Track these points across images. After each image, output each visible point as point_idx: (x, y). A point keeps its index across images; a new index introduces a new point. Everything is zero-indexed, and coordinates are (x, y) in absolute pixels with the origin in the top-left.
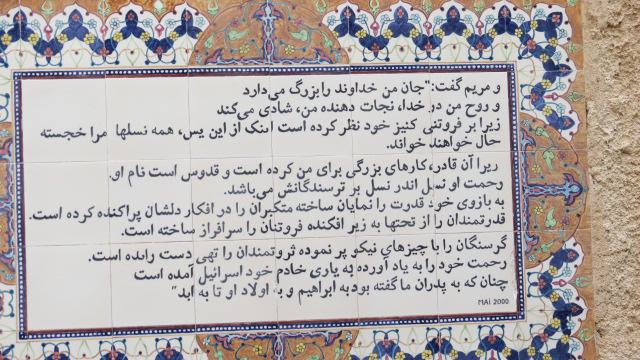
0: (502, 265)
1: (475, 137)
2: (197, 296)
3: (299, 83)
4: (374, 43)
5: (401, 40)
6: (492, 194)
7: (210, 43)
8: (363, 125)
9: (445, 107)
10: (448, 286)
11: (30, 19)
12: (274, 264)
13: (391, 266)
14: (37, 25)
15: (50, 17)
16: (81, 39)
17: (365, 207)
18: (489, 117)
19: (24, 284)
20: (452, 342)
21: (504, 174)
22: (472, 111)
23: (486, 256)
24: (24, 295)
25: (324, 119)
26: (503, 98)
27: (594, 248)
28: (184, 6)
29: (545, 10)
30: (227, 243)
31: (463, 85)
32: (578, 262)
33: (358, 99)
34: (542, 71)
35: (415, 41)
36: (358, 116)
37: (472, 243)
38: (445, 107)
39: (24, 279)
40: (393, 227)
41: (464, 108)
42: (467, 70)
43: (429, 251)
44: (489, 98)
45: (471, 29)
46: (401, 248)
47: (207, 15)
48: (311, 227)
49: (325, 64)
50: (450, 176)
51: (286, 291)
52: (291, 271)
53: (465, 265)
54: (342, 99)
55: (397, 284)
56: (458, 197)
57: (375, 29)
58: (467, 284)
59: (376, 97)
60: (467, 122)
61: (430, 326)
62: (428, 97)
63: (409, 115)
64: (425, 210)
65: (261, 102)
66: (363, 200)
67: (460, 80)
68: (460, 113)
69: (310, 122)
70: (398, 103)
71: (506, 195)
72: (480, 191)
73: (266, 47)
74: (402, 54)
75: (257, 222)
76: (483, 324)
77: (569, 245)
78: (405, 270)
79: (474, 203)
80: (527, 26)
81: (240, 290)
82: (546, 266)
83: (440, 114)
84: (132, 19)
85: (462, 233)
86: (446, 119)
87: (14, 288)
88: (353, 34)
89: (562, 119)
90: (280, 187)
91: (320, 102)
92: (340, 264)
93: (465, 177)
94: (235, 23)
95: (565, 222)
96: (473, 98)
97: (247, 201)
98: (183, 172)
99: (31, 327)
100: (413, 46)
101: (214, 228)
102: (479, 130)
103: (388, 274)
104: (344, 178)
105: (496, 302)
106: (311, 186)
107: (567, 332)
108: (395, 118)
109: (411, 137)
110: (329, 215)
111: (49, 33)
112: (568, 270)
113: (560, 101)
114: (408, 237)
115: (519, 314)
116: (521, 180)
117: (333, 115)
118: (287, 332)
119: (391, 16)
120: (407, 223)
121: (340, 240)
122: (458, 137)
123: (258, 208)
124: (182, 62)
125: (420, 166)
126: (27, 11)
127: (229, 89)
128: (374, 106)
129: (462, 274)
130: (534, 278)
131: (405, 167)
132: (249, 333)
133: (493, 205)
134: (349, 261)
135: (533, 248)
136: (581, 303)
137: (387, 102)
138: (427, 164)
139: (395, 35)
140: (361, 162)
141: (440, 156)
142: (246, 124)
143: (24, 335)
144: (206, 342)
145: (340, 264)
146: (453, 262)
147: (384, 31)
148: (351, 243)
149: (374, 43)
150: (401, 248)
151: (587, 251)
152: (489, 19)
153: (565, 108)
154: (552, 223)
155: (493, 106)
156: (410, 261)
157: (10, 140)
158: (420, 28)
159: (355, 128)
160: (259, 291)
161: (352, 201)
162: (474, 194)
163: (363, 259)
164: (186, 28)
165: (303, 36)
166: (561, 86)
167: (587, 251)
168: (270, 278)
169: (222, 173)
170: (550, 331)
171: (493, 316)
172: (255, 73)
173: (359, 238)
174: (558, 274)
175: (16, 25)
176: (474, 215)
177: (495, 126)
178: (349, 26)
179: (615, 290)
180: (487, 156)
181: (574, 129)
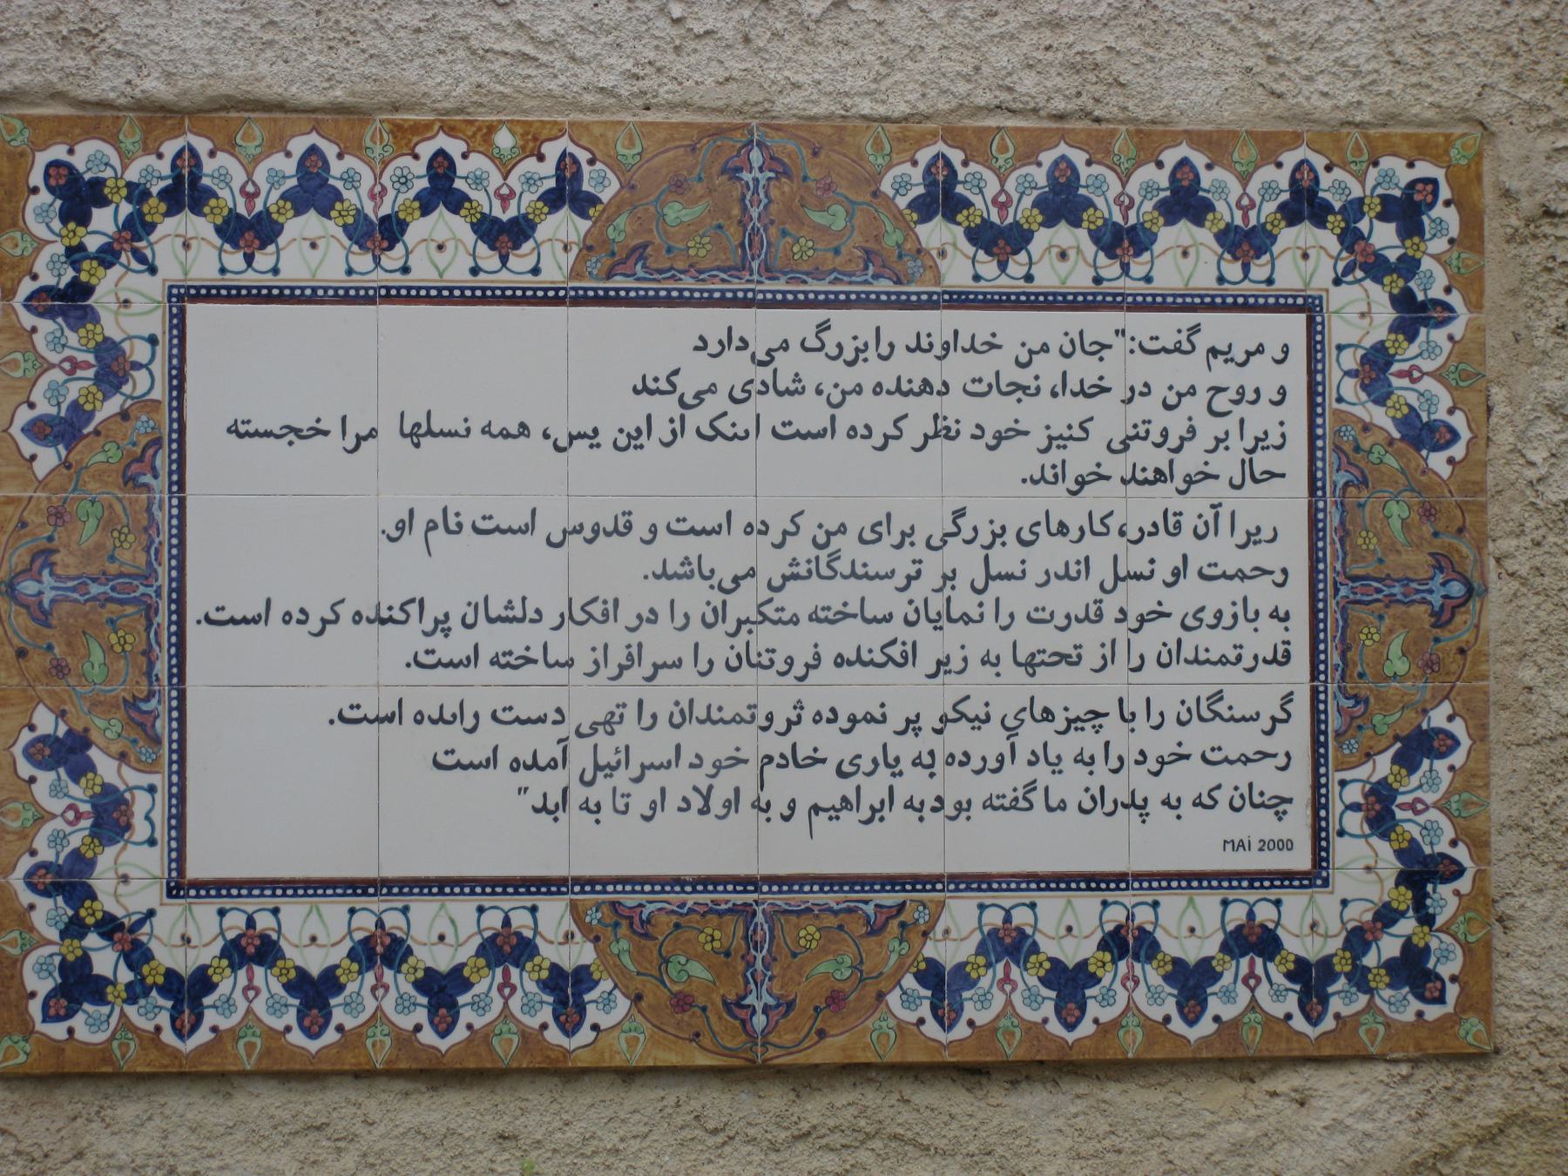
0: (1282, 761)
1: (1227, 464)
3: (824, 327)
5: (1063, 234)
6: (1262, 594)
7: (621, 230)
8: (967, 429)
9: (1159, 392)
10: (1154, 807)
11: (209, 165)
12: (748, 740)
13: (1023, 755)
14: (224, 177)
15: (256, 160)
16: (325, 213)
17: (966, 619)
18: (1260, 418)
19: (182, 773)
20: (1159, 935)
21: (1292, 552)
22: (1221, 403)
23: (1246, 739)
24: (179, 798)
25: (878, 412)
26: (1295, 375)
27: (1498, 724)
28: (564, 143)
29: (1399, 173)
30: (647, 693)
31: (1203, 342)
32: (1458, 758)
33: (960, 368)
34: (1385, 314)
35: (1095, 237)
36: (956, 407)
37: (1211, 709)
38: (1159, 392)
39: (182, 761)
40: (1030, 665)
41: (1203, 396)
42: (1212, 307)
43: (1112, 724)
44: (1262, 374)
45: (1225, 212)
46: (1048, 715)
47: (615, 165)
48: (840, 661)
49: (884, 285)
50: (1166, 551)
51: (780, 807)
52: (792, 760)
53: (1196, 759)
54: (923, 367)
55: (1037, 797)
56: (1183, 599)
57: (1003, 207)
58: (1198, 803)
59: (1002, 363)
60: (1209, 428)
61: (1110, 896)
62: (1118, 369)
63: (1073, 409)
64: (1108, 629)
65: (735, 369)
66: (964, 602)
67: (1195, 329)
68: (1194, 406)
69: (845, 419)
70: (1050, 380)
71: (1296, 598)
72: (1236, 589)
73: (749, 242)
74: (1063, 268)
75: (717, 644)
76: (1231, 895)
77: (1438, 717)
78: (1055, 766)
79: (1219, 615)
80: (1355, 209)
81: (673, 801)
82: (1383, 766)
83: (1145, 408)
84: (441, 168)
85: (1192, 682)
86: (1161, 419)
87: (156, 779)
88: (951, 217)
89: (1431, 427)
90: (773, 565)
91: (871, 371)
92: (905, 748)
93: (1201, 554)
94: (678, 187)
95: (1431, 666)
96: (1224, 373)
97: (694, 597)
99: (194, 871)
100: (1089, 248)
101: (618, 656)
102: (1237, 447)
104: (920, 551)
105: (1264, 845)
106: (843, 566)
107: (1426, 920)
109: (1080, 458)
110: (883, 633)
111: (250, 197)
112: (1432, 781)
113: (1428, 384)
115: (1317, 875)
116: (1331, 565)
117: (899, 404)
118: (781, 900)
119: (1040, 176)
120: (1063, 657)
122: (1188, 462)
123: (720, 613)
124: (555, 271)
125: (1098, 527)
126: (202, 146)
128: (995, 386)
129: (1187, 780)
130: (1354, 794)
131: (1063, 529)
132: (691, 899)
133: (1264, 621)
134: (928, 740)
135: (1354, 724)
136: (1461, 854)
137: (1024, 377)
138: (1114, 523)
139: (1049, 223)
140: (960, 513)
141: (1145, 506)
142: (698, 418)
143: (178, 888)
144: (593, 918)
145: (905, 748)
147: (1024, 209)
148: (933, 701)
150: (1048, 715)
151: (1480, 734)
152: (1268, 189)
153: (1439, 403)
154: (1401, 666)
155: (1270, 393)
156: (1067, 746)
157: (157, 442)
158: (1106, 208)
159: (950, 435)
160: (716, 806)
161: (936, 604)
162: (1221, 596)
163: (959, 737)
165: (836, 218)
166: (1430, 350)
167: (1480, 734)
168: (745, 777)
169: (640, 529)
170: (1386, 916)
171: (1255, 879)
172: (723, 302)
173: (952, 689)
174: (1411, 786)
175: (178, 179)
176: (1218, 643)
177: (1275, 439)
179: (1541, 825)
180: (1254, 508)
181: (1458, 451)
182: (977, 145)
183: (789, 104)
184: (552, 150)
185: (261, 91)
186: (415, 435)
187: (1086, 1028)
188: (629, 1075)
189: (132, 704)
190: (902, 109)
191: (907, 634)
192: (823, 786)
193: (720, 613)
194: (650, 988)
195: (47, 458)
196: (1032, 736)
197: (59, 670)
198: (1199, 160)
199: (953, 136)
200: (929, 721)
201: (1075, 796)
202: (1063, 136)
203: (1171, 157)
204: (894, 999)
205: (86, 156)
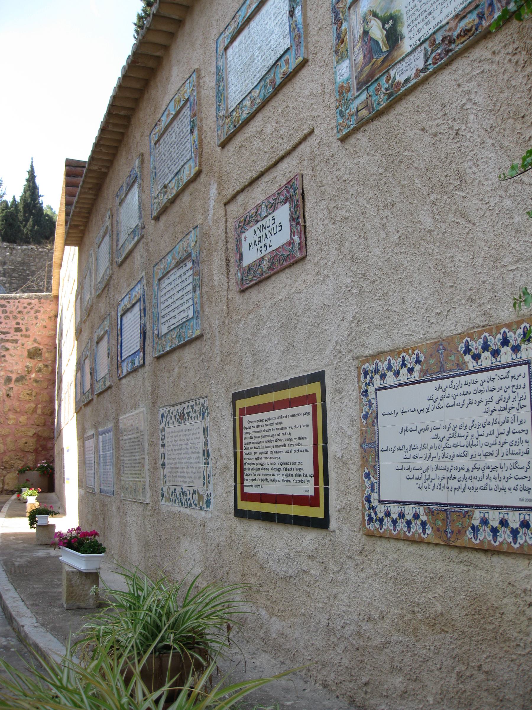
0: (528, 479)
1: (516, 404)
2: (423, 489)
3: (452, 382)
8: (474, 402)
10: (507, 490)
20: (509, 522)
22: (514, 390)
25: (460, 399)
30: (432, 463)
31: (510, 375)
37: (515, 466)
38: (504, 388)
40: (485, 456)
41: (511, 388)
45: (512, 343)
46: (488, 468)
47: (424, 354)
49: (460, 371)
50: (506, 426)
51: (450, 489)
53: (513, 478)
54: (465, 389)
60: (513, 396)
62: (497, 384)
63: (489, 395)
64: (498, 447)
65: (440, 393)
67: (509, 372)
68: (509, 391)
70: (486, 388)
79: (516, 442)
83: (502, 392)
84: (403, 360)
85: (510, 460)
91: (460, 391)
96: (515, 382)
97: (437, 442)
98: (419, 430)
100: (490, 356)
102: (518, 399)
103: (485, 481)
108: (486, 396)
109: (492, 406)
114: (492, 462)
119: (481, 341)
121: (467, 463)
123: (440, 446)
124: (417, 378)
127: (429, 388)
129: (512, 483)
133: (524, 444)
138: (497, 421)
140: (473, 421)
141: (501, 416)
142: (436, 404)
143: (380, 501)
146: (507, 476)
149: (476, 357)
155: (522, 386)
156: (492, 475)
164: (418, 361)
165: (452, 358)
168: (444, 481)
169: (430, 430)
173: (474, 461)
176: (515, 449)
177: (524, 397)
178: (467, 351)
183: (445, 334)
184: (415, 352)
185: (382, 350)
186: (403, 412)
187: (497, 543)
188: (429, 544)
189: (374, 466)
190: (459, 331)
191: (467, 449)
192: (454, 484)
193: (440, 446)
194: (434, 526)
195: (365, 421)
196: (487, 472)
197: (367, 461)
198: (507, 330)
199: (468, 335)
200: (471, 469)
201: (494, 487)
202: (485, 331)
203: (502, 331)
204: (468, 532)
205: (366, 366)
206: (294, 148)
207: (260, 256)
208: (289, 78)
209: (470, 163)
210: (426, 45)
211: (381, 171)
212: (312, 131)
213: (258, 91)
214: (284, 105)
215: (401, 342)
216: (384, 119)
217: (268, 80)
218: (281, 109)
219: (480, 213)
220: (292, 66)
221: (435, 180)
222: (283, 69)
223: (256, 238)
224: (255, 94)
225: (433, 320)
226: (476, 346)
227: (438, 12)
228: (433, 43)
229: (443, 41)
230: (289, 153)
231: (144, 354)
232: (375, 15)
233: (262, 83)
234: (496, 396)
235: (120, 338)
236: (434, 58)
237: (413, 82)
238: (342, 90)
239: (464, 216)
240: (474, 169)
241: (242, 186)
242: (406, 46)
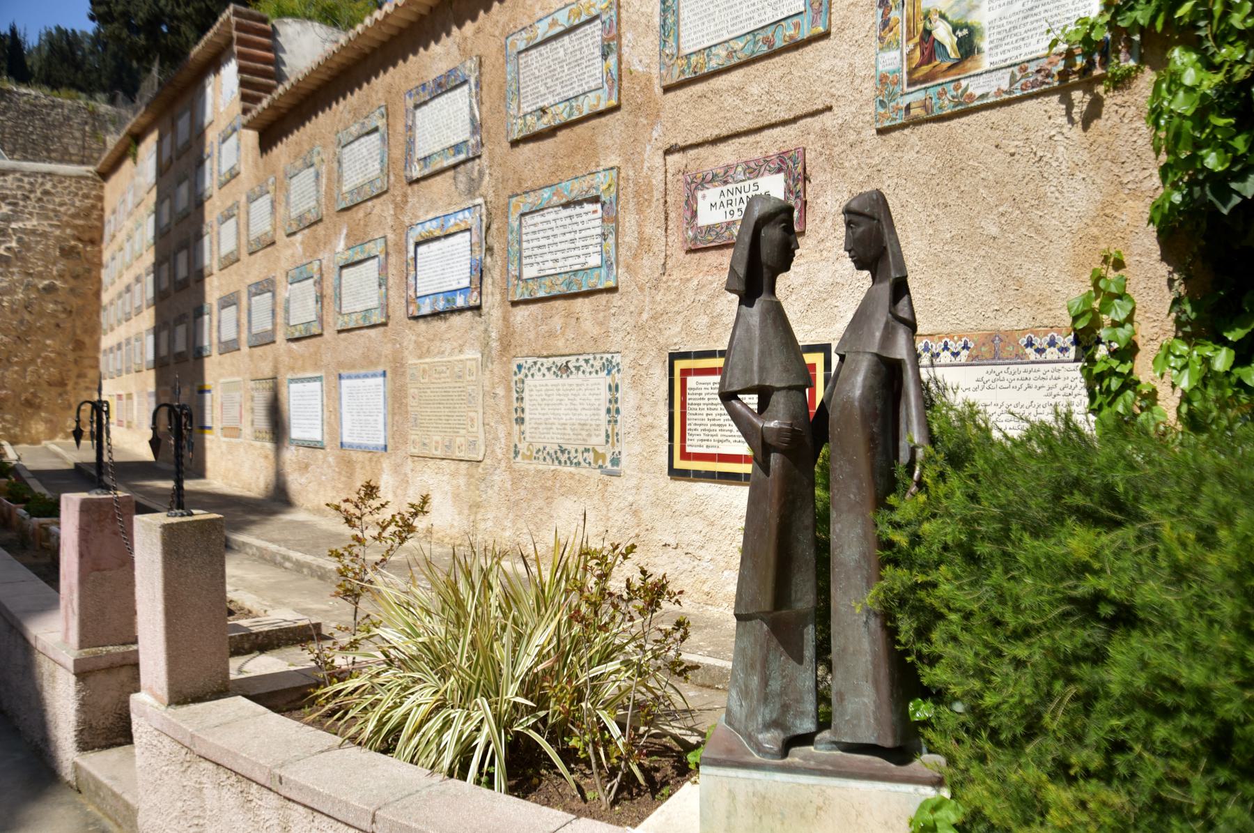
4: (1040, 351)
5: (1052, 349)
7: (974, 353)
25: (1018, 384)
33: (1033, 375)
36: (1032, 382)
54: (1025, 375)
59: (1040, 374)
62: (1063, 374)
63: (1053, 382)
65: (993, 376)
73: (996, 353)
83: (1068, 381)
84: (946, 344)
90: (999, 411)
91: (1016, 376)
108: (1047, 383)
109: (1054, 391)
122: (1076, 392)
124: (963, 361)
147: (1045, 345)
149: (1040, 351)
164: (965, 347)
165: (1010, 348)
178: (1030, 344)
182: (1036, 334)
206: (795, 120)
207: (729, 218)
208: (796, 45)
209: (1053, 189)
210: (1016, 69)
211: (933, 171)
212: (829, 109)
213: (741, 45)
214: (786, 70)
215: (946, 328)
216: (946, 124)
217: (760, 37)
218: (778, 73)
219: (1059, 233)
220: (805, 33)
221: (1006, 195)
222: (789, 31)
223: (724, 200)
224: (738, 45)
225: (989, 314)
226: (1039, 342)
227: (1034, 41)
228: (1024, 70)
229: (1038, 71)
230: (784, 123)
231: (481, 294)
232: (943, 16)
233: (749, 37)
234: (1061, 384)
235: (411, 268)
236: (1025, 84)
237: (991, 100)
238: (883, 79)
239: (1037, 231)
240: (1057, 194)
241: (700, 140)
242: (985, 62)
